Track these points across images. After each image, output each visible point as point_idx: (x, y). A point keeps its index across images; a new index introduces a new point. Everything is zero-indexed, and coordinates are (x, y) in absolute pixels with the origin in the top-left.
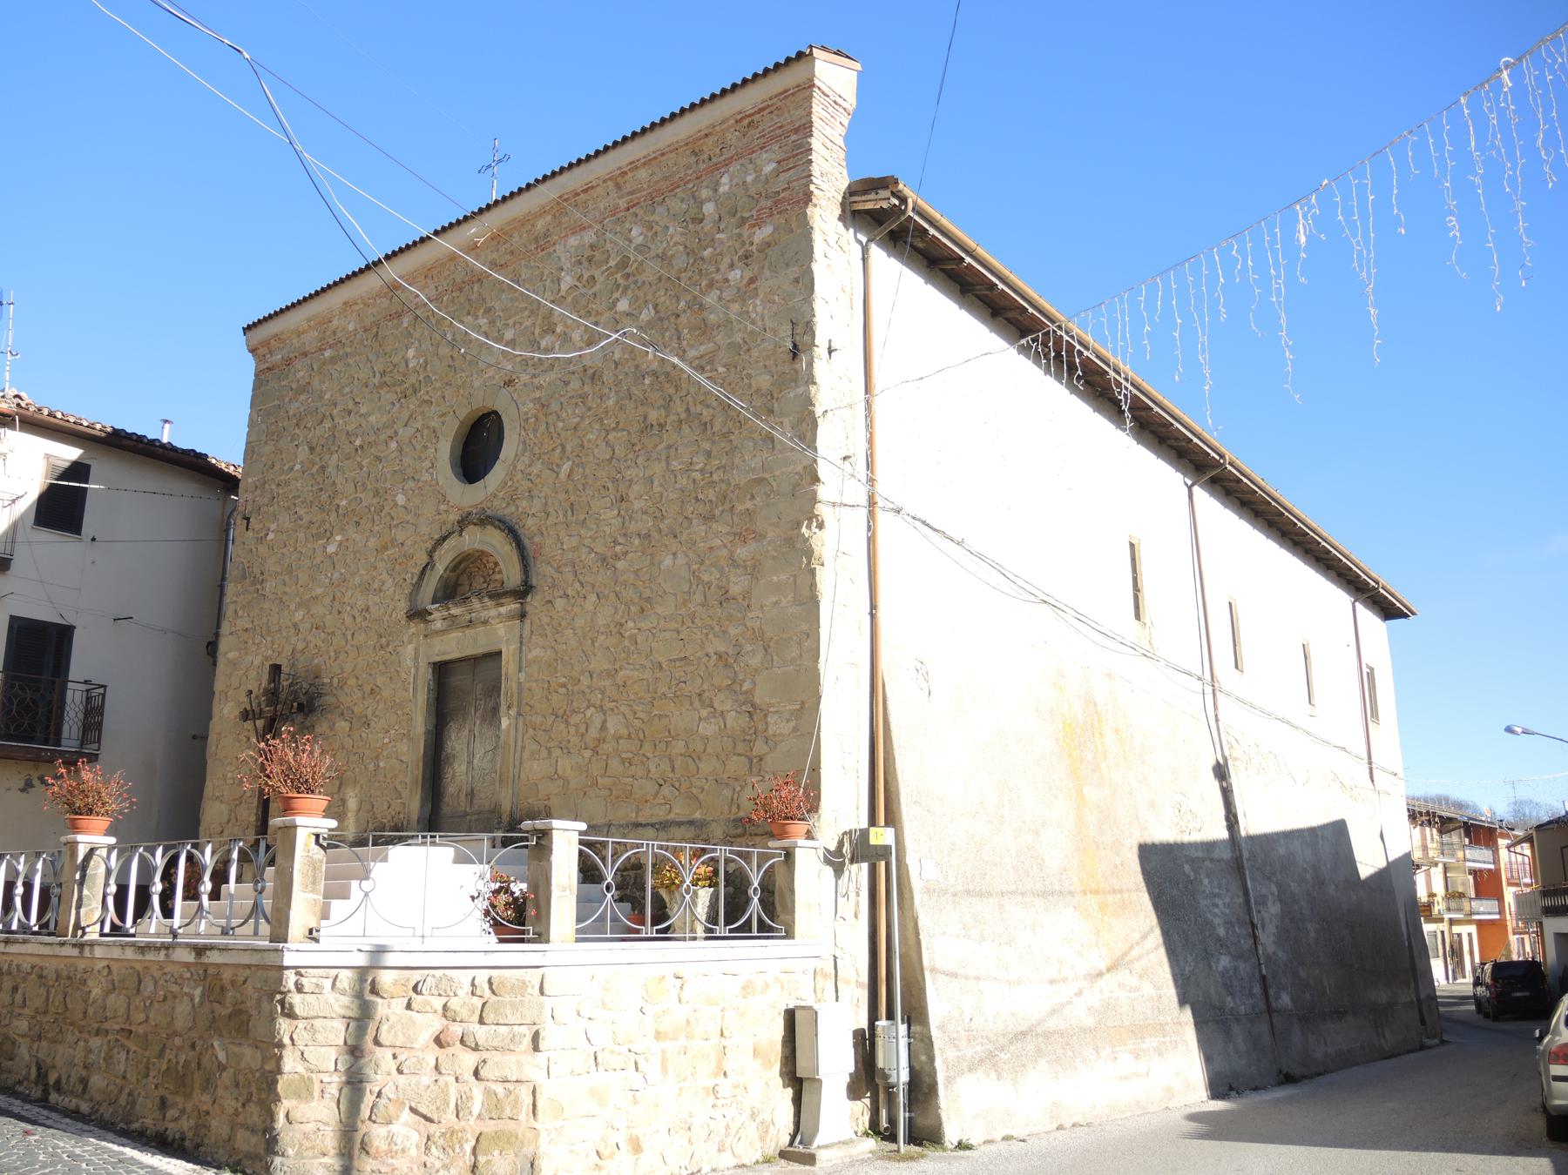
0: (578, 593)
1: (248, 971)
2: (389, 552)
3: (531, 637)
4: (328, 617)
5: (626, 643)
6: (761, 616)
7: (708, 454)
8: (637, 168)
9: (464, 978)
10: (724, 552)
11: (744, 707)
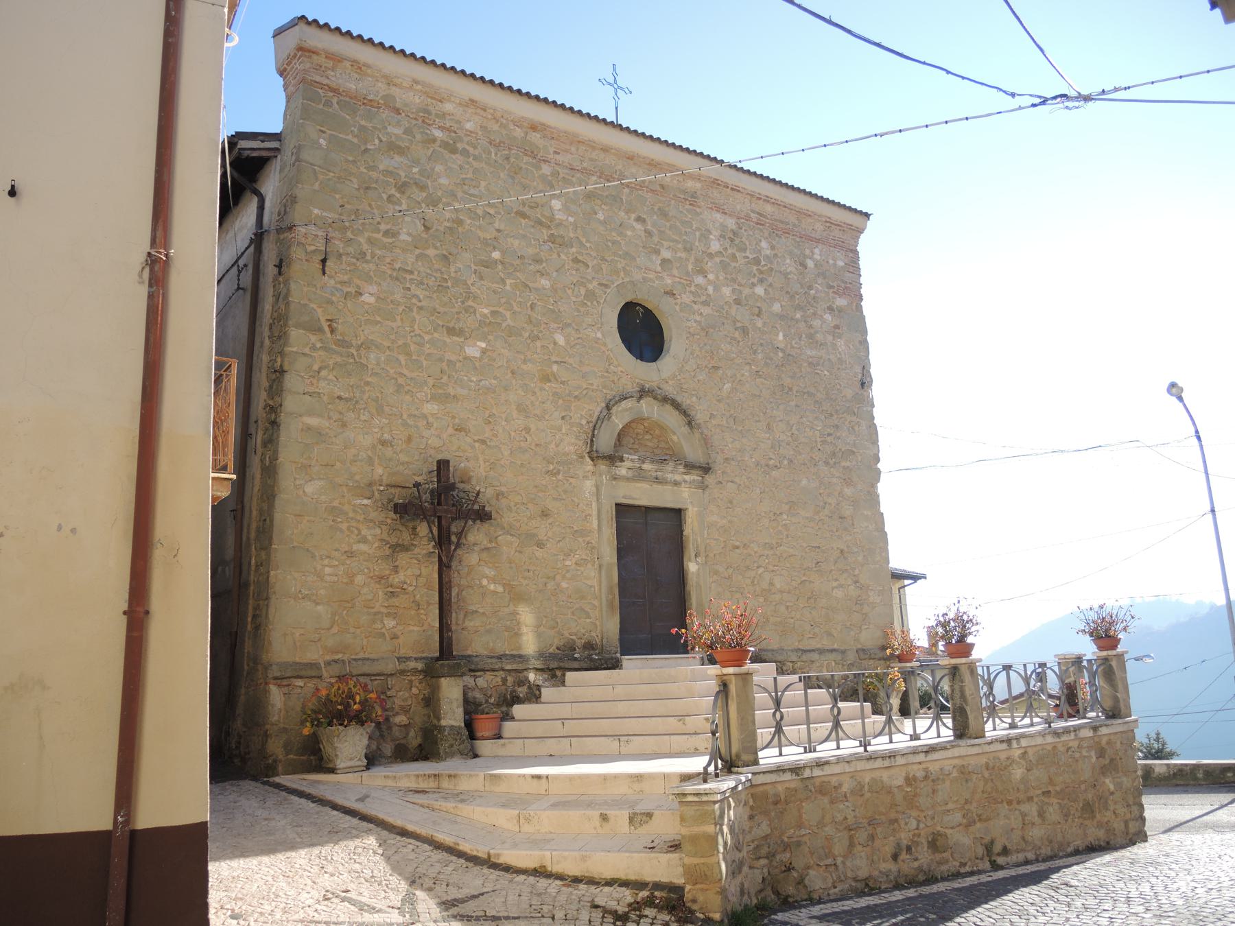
8: (768, 201)
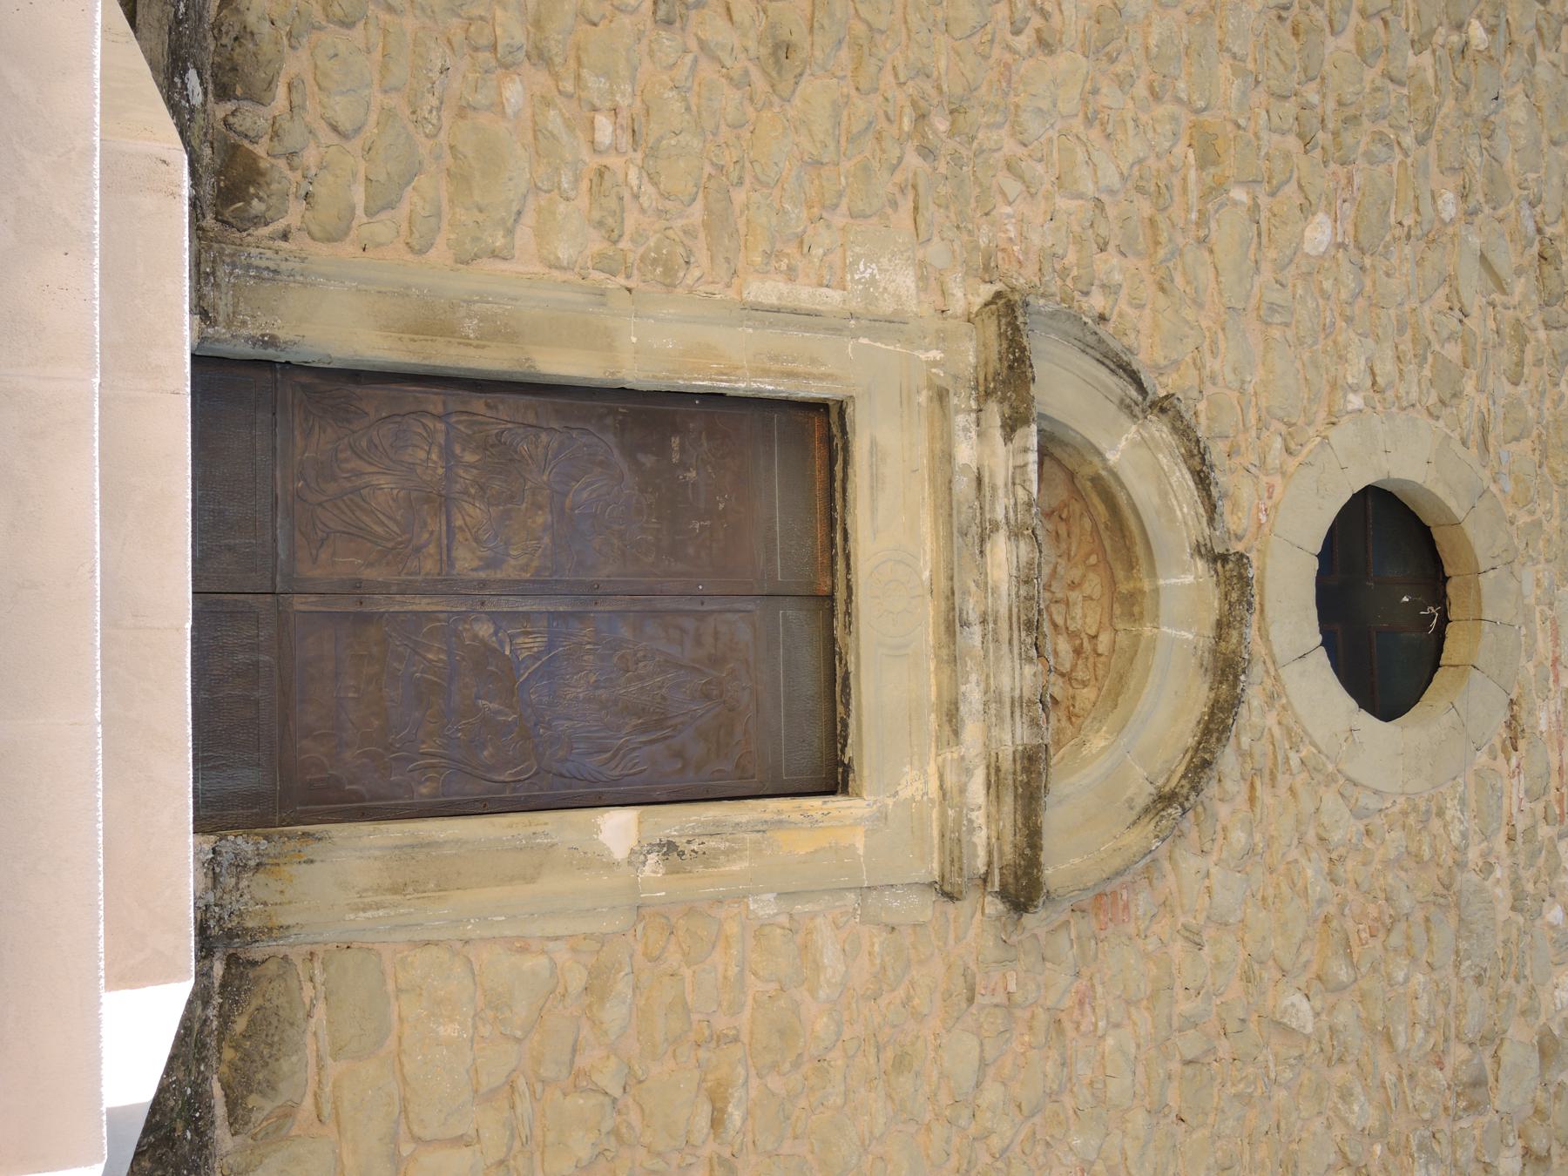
0: (984, 1136)
2: (1192, 175)
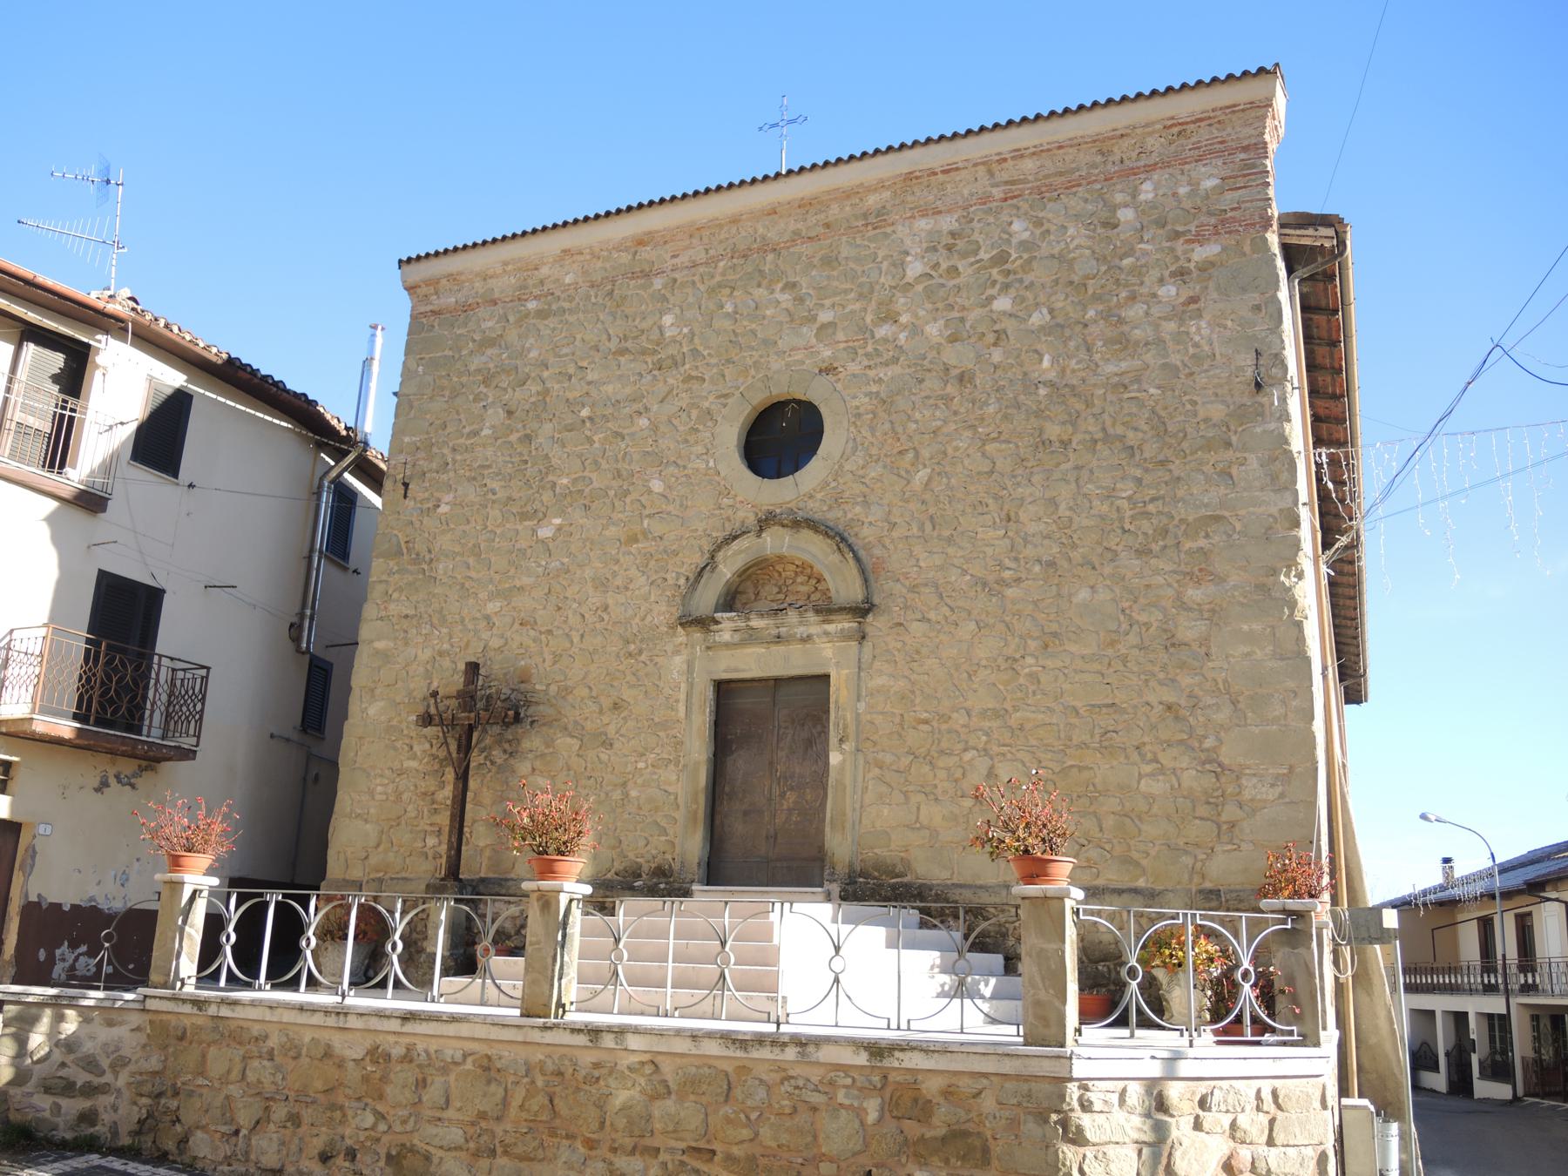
0: (946, 618)
1: (985, 1082)
2: (640, 545)
3: (872, 663)
4: (541, 612)
5: (1022, 680)
6: (1226, 666)
7: (1139, 481)
8: (1022, 156)
9: (1249, 1089)
10: (1170, 592)
11: (1208, 767)
